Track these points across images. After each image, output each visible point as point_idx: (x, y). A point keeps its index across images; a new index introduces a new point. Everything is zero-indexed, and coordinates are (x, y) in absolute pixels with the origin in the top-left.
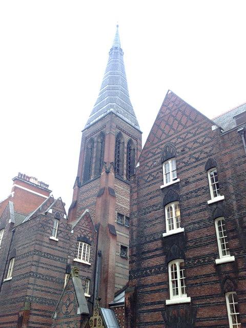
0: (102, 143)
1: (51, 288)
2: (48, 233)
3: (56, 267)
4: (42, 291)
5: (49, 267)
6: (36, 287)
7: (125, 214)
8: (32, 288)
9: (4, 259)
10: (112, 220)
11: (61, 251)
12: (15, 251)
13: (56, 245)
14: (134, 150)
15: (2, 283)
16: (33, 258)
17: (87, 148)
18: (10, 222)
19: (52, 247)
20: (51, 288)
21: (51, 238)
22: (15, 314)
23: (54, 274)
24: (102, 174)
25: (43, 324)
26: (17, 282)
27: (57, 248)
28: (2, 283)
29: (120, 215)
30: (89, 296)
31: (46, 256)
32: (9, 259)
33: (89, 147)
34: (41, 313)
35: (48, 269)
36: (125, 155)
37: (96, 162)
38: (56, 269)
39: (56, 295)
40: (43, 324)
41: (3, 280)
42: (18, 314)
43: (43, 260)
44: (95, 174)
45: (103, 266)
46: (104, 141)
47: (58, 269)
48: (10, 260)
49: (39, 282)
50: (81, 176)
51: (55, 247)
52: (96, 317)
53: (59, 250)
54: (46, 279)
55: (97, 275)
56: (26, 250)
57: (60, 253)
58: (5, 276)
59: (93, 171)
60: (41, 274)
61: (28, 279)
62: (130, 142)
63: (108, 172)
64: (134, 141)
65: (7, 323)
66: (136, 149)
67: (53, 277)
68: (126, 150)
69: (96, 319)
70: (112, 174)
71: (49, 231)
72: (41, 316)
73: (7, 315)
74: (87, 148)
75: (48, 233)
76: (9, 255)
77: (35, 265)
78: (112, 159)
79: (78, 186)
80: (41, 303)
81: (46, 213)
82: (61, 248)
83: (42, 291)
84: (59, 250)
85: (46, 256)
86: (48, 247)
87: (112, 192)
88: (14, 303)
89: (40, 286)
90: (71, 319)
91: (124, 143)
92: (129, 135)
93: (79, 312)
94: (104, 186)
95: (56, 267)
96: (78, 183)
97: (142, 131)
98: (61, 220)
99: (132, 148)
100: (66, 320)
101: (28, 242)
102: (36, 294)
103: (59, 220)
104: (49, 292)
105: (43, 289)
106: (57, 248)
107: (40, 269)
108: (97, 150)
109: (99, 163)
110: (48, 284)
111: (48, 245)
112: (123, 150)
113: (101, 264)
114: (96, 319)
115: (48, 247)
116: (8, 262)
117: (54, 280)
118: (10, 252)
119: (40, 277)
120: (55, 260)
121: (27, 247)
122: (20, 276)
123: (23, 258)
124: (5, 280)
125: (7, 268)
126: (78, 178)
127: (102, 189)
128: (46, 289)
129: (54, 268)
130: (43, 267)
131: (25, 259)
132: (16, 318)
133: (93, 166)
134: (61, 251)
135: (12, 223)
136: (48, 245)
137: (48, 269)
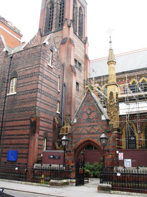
0: (61, 5)
1: (50, 103)
2: (47, 60)
3: (52, 87)
4: (45, 104)
5: (48, 87)
6: (41, 101)
7: (78, 60)
8: (39, 101)
9: (4, 79)
10: (73, 63)
11: (55, 76)
12: (15, 73)
13: (51, 71)
14: (82, 15)
15: (6, 97)
16: (38, 77)
17: (47, 8)
18: (4, 50)
19: (50, 71)
20: (50, 103)
21: (48, 64)
22: (26, 120)
23: (51, 93)
24: (64, 27)
25: (47, 128)
26: (23, 96)
27: (52, 73)
28: (6, 97)
29: (76, 61)
30: (59, 113)
31: (46, 78)
32: (9, 78)
33: (49, 7)
34: (45, 120)
35: (48, 88)
36: (78, 17)
37: (56, 18)
38: (52, 89)
39: (53, 108)
40: (47, 128)
41: (6, 95)
42: (30, 119)
43: (45, 81)
44: (55, 27)
45: (67, 94)
46: (63, 3)
47: (54, 90)
48: (11, 79)
49: (43, 97)
50: (43, 29)
51: (51, 72)
52: (67, 127)
53: (53, 75)
54: (47, 96)
55: (63, 99)
56: (29, 72)
57: (54, 77)
58: (7, 91)
59: (54, 26)
60: (44, 92)
61: (35, 94)
62: (80, 8)
63: (69, 27)
64: (83, 8)
65: (17, 126)
66: (84, 15)
67: (51, 95)
68: (78, 14)
69: (67, 128)
70: (72, 29)
71: (47, 58)
72: (46, 122)
73: (16, 121)
74: (47, 8)
75: (47, 60)
76: (10, 76)
77: (40, 84)
78: (71, 18)
79: (41, 36)
80: (45, 113)
81: (45, 44)
82: (55, 73)
83: (45, 104)
84: (53, 75)
85: (46, 78)
86: (47, 71)
87: (71, 41)
88: (22, 111)
89: (44, 100)
90: (95, 124)
91: (77, 8)
92: (80, 3)
93: (103, 118)
94: (66, 36)
95: (52, 87)
96: (40, 32)
97: (87, 3)
98: (54, 52)
99: (81, 14)
100: (89, 124)
101: (30, 65)
102: (42, 106)
103: (52, 52)
104: (49, 106)
105: (46, 103)
106: (52, 73)
107: (43, 87)
108: (57, 10)
109: (58, 20)
110: (48, 99)
111: (47, 70)
112: (77, 14)
113: (66, 92)
114: (67, 128)
115: (47, 71)
116: (9, 81)
117: (52, 97)
118: (10, 73)
119: (43, 94)
120: (51, 82)
121: (30, 69)
122: (25, 91)
123: (22, 79)
124: (8, 95)
125: (8, 86)
126: (40, 29)
127: (65, 39)
128: (48, 103)
129: (51, 88)
130: (45, 86)
131: (28, 78)
132: (28, 122)
133: (54, 21)
134: (55, 76)
135: (7, 52)
136: (47, 70)
137: (48, 88)
